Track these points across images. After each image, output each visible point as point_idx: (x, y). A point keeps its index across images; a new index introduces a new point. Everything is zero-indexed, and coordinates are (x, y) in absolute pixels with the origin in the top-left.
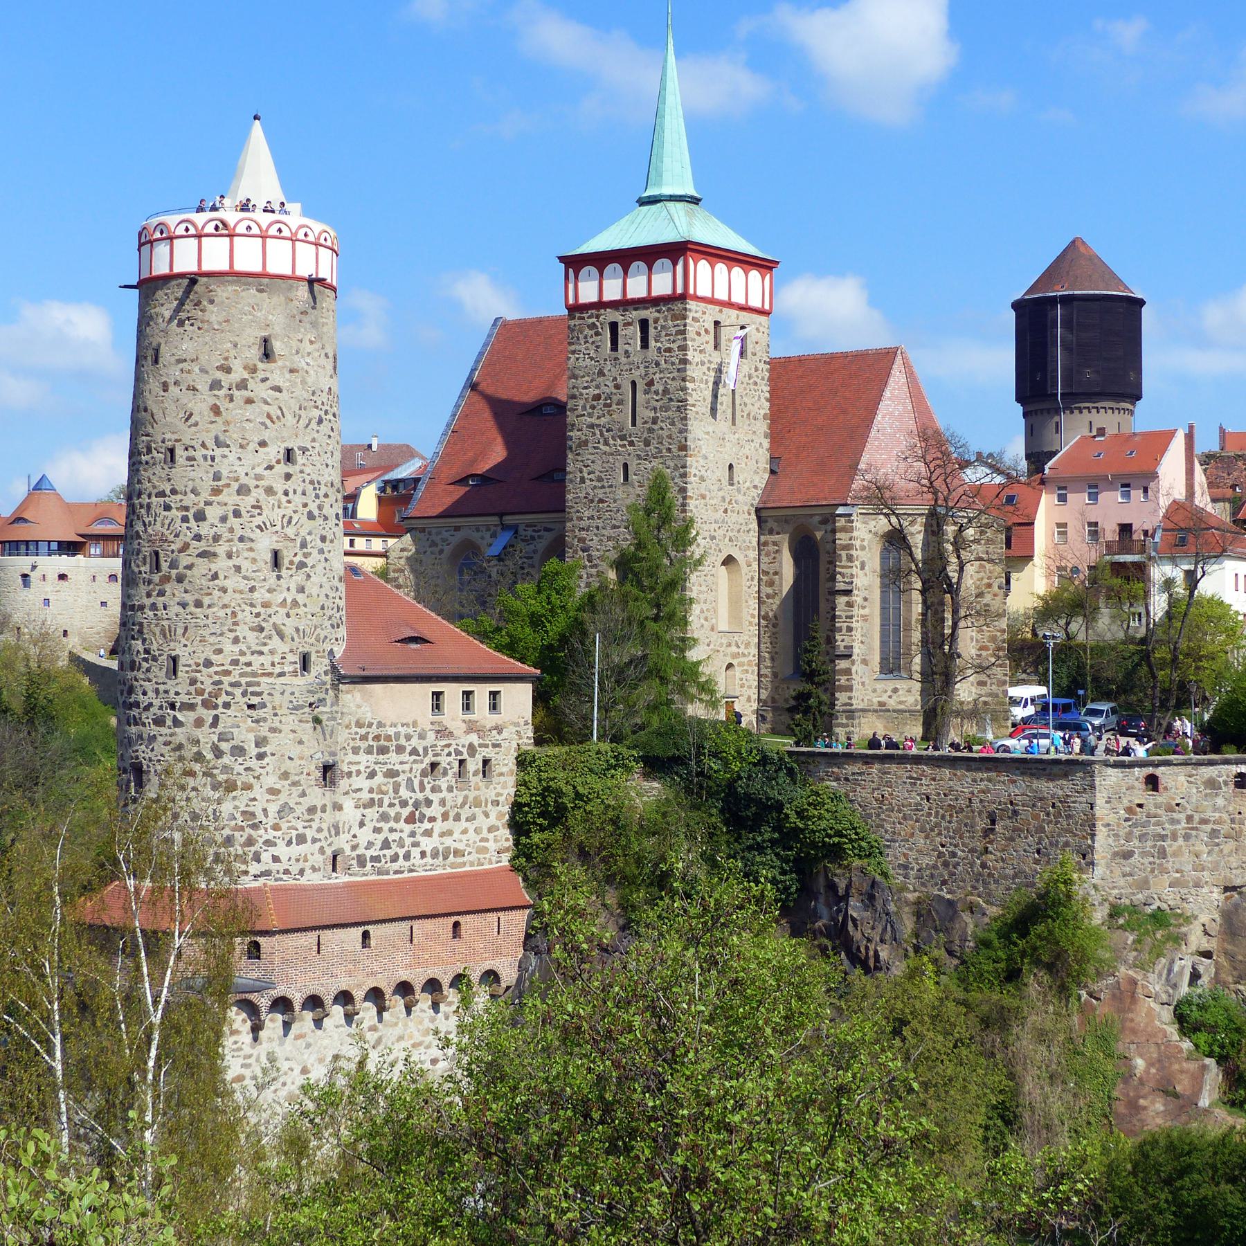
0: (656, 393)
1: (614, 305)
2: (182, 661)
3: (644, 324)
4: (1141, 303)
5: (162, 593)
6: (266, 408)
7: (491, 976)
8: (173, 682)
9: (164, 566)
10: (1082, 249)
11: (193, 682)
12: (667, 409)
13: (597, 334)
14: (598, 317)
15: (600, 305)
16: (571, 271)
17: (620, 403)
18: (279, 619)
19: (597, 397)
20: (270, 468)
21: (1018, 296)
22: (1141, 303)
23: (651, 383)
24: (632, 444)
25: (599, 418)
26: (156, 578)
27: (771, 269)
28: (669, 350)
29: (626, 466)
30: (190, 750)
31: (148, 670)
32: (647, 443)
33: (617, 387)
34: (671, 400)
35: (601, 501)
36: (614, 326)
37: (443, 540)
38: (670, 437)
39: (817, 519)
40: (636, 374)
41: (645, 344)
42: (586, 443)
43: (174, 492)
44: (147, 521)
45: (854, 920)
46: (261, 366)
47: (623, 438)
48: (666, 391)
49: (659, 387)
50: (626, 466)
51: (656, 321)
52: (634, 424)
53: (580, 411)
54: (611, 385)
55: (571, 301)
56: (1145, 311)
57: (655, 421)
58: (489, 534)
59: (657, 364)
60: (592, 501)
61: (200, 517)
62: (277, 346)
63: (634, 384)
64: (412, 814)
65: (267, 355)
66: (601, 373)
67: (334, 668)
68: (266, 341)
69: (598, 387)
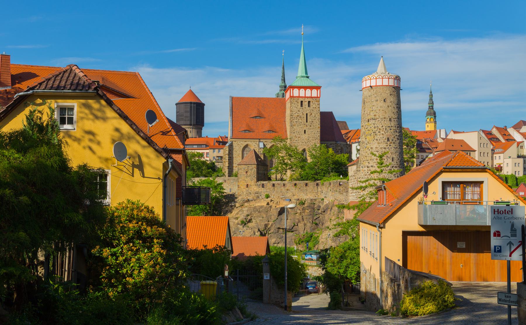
0: (313, 116)
1: (302, 97)
2: (395, 158)
3: (309, 102)
5: (390, 146)
8: (393, 163)
9: (391, 141)
11: (397, 162)
12: (315, 120)
13: (298, 103)
14: (298, 99)
15: (299, 97)
16: (291, 89)
17: (303, 117)
19: (298, 116)
23: (311, 114)
24: (307, 126)
25: (298, 120)
26: (389, 143)
28: (316, 108)
29: (305, 131)
30: (396, 176)
31: (387, 160)
32: (310, 126)
33: (303, 114)
34: (316, 118)
35: (299, 137)
36: (302, 102)
37: (241, 144)
38: (316, 125)
39: (329, 144)
40: (308, 112)
41: (309, 106)
42: (295, 125)
44: (386, 132)
47: (305, 125)
48: (315, 116)
49: (313, 115)
50: (305, 131)
51: (313, 102)
52: (307, 122)
53: (293, 118)
54: (302, 114)
55: (292, 95)
56: (205, 106)
57: (312, 122)
58: (254, 143)
59: (313, 110)
60: (296, 137)
63: (307, 114)
66: (299, 111)
69: (298, 114)
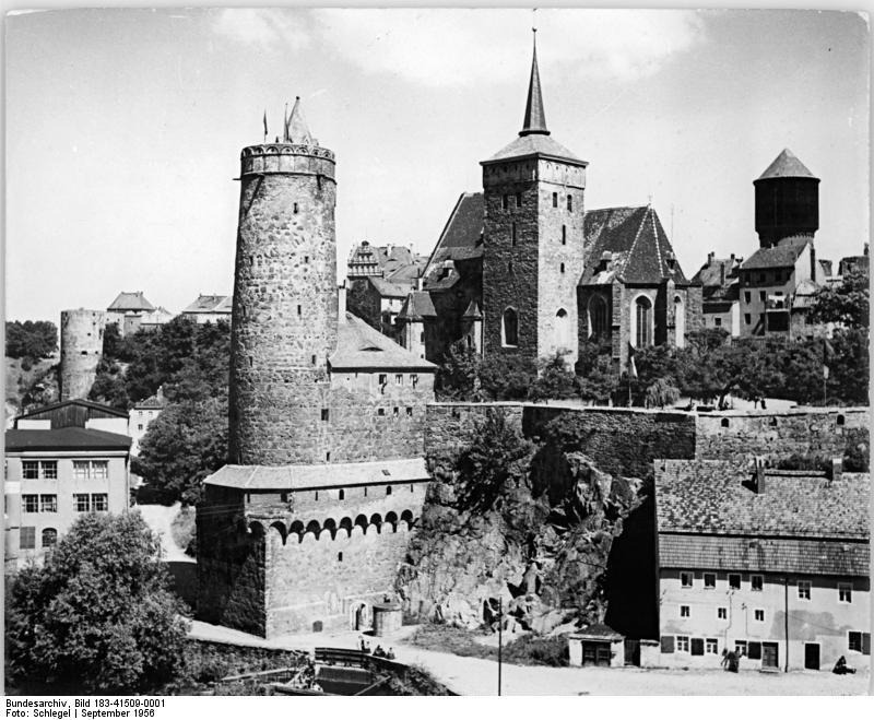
4: (818, 181)
6: (295, 237)
7: (407, 515)
10: (789, 155)
18: (301, 339)
20: (297, 266)
21: (757, 178)
22: (818, 181)
27: (584, 167)
43: (253, 278)
45: (580, 489)
46: (293, 216)
61: (264, 291)
62: (301, 207)
64: (369, 435)
65: (296, 212)
67: (328, 364)
68: (295, 204)
